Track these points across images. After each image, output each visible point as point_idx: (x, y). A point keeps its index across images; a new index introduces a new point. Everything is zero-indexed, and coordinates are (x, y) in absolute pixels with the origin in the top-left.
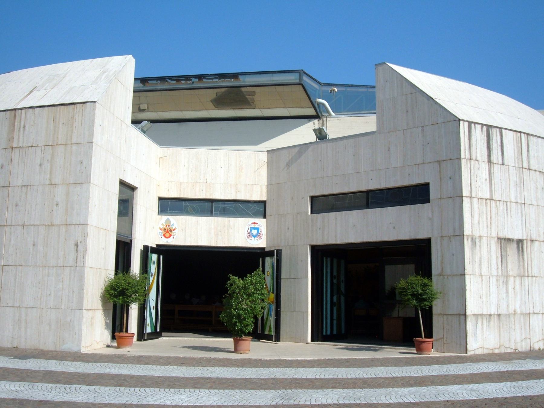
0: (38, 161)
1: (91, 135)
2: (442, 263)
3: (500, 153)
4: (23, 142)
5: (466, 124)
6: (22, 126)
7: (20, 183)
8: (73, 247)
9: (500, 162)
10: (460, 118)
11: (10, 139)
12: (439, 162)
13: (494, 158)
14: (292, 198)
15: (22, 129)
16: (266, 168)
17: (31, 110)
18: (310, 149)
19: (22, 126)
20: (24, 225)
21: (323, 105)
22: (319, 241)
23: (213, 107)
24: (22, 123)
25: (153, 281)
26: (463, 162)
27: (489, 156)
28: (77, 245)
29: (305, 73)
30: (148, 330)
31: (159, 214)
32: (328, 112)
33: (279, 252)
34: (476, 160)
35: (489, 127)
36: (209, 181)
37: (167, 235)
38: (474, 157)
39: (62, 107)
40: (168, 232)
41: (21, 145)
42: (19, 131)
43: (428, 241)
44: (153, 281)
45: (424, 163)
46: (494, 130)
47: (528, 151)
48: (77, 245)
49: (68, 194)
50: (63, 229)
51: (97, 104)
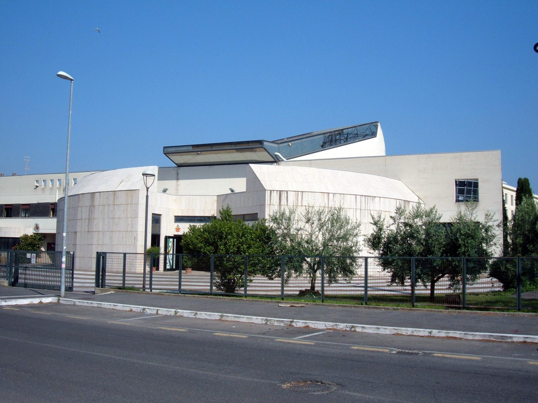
1: (138, 201)
3: (286, 201)
5: (269, 192)
7: (117, 217)
8: (133, 238)
9: (286, 204)
10: (266, 189)
11: (114, 202)
13: (282, 203)
16: (216, 203)
21: (278, 155)
25: (171, 249)
26: (267, 206)
27: (280, 202)
28: (135, 238)
29: (265, 141)
30: (168, 267)
31: (175, 222)
32: (281, 159)
34: (273, 205)
35: (280, 191)
36: (193, 209)
37: (178, 231)
38: (272, 203)
40: (178, 229)
44: (171, 249)
46: (283, 192)
47: (302, 198)
48: (135, 238)
50: (131, 232)
51: (140, 190)
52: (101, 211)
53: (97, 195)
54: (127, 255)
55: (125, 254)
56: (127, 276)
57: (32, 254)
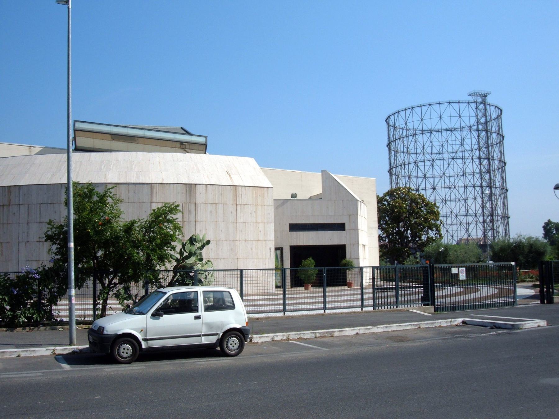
0: (250, 212)
2: (350, 254)
4: (241, 202)
6: (240, 194)
7: (242, 221)
8: (269, 250)
12: (349, 215)
14: (280, 224)
15: (240, 196)
17: (244, 187)
18: (289, 202)
19: (240, 194)
20: (246, 240)
22: (295, 244)
23: (111, 139)
24: (240, 193)
33: (282, 248)
39: (258, 188)
41: (240, 203)
42: (239, 196)
43: (344, 246)
45: (343, 215)
48: (270, 249)
49: (265, 227)
50: (264, 242)
52: (211, 212)
53: (200, 189)
54: (244, 272)
55: (241, 271)
56: (90, 305)
57: (460, 269)
